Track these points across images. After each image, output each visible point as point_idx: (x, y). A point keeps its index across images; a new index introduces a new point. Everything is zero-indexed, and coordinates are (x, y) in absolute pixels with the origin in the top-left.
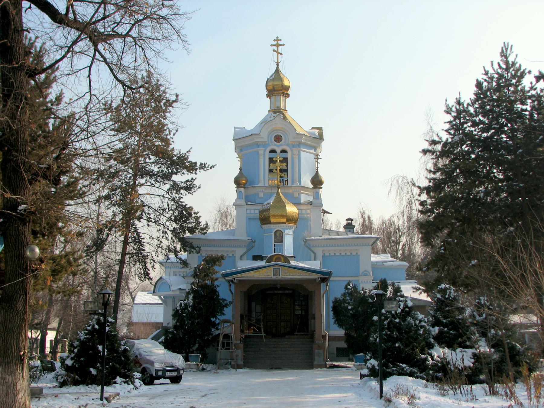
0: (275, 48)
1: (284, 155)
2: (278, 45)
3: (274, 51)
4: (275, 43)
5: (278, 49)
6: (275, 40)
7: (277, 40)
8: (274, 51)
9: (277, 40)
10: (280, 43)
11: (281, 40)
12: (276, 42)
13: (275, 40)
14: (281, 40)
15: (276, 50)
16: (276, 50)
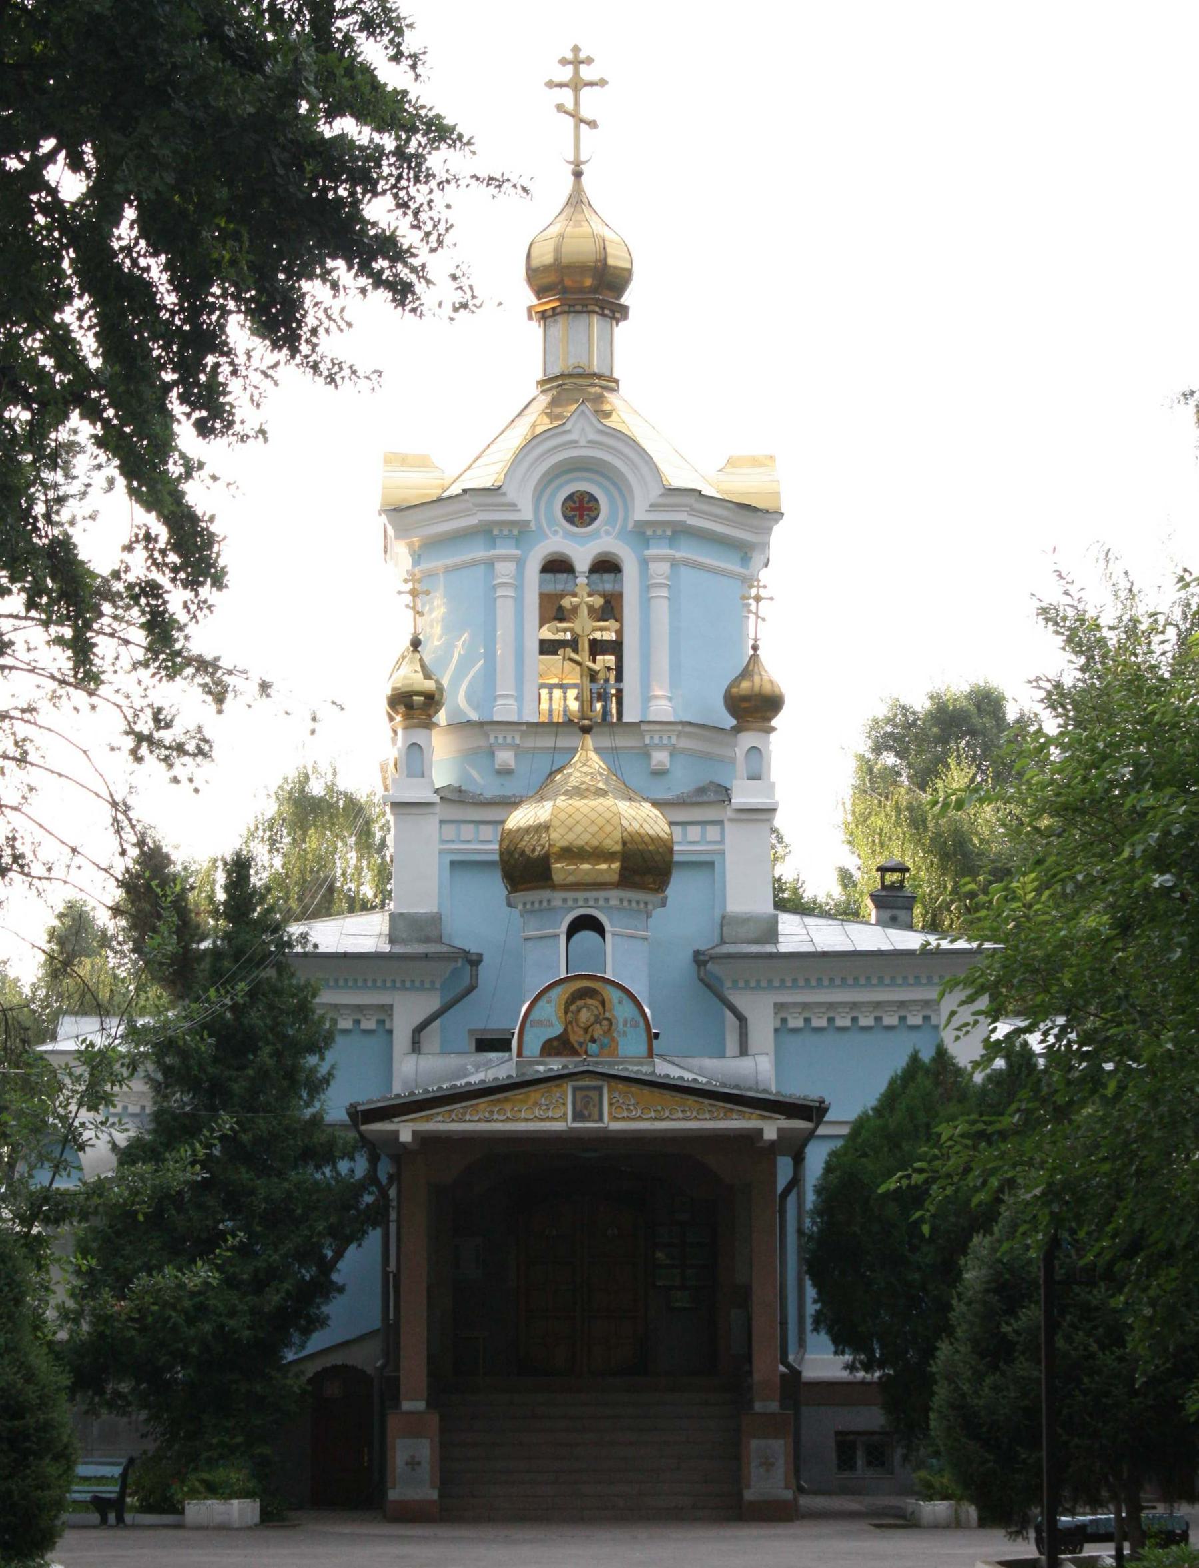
0: (566, 96)
1: (607, 583)
2: (576, 85)
3: (560, 108)
4: (566, 73)
5: (576, 102)
6: (564, 62)
7: (576, 61)
8: (560, 108)
9: (576, 61)
10: (586, 73)
11: (589, 61)
12: (570, 68)
13: (564, 62)
14: (589, 61)
15: (570, 106)
16: (570, 106)
